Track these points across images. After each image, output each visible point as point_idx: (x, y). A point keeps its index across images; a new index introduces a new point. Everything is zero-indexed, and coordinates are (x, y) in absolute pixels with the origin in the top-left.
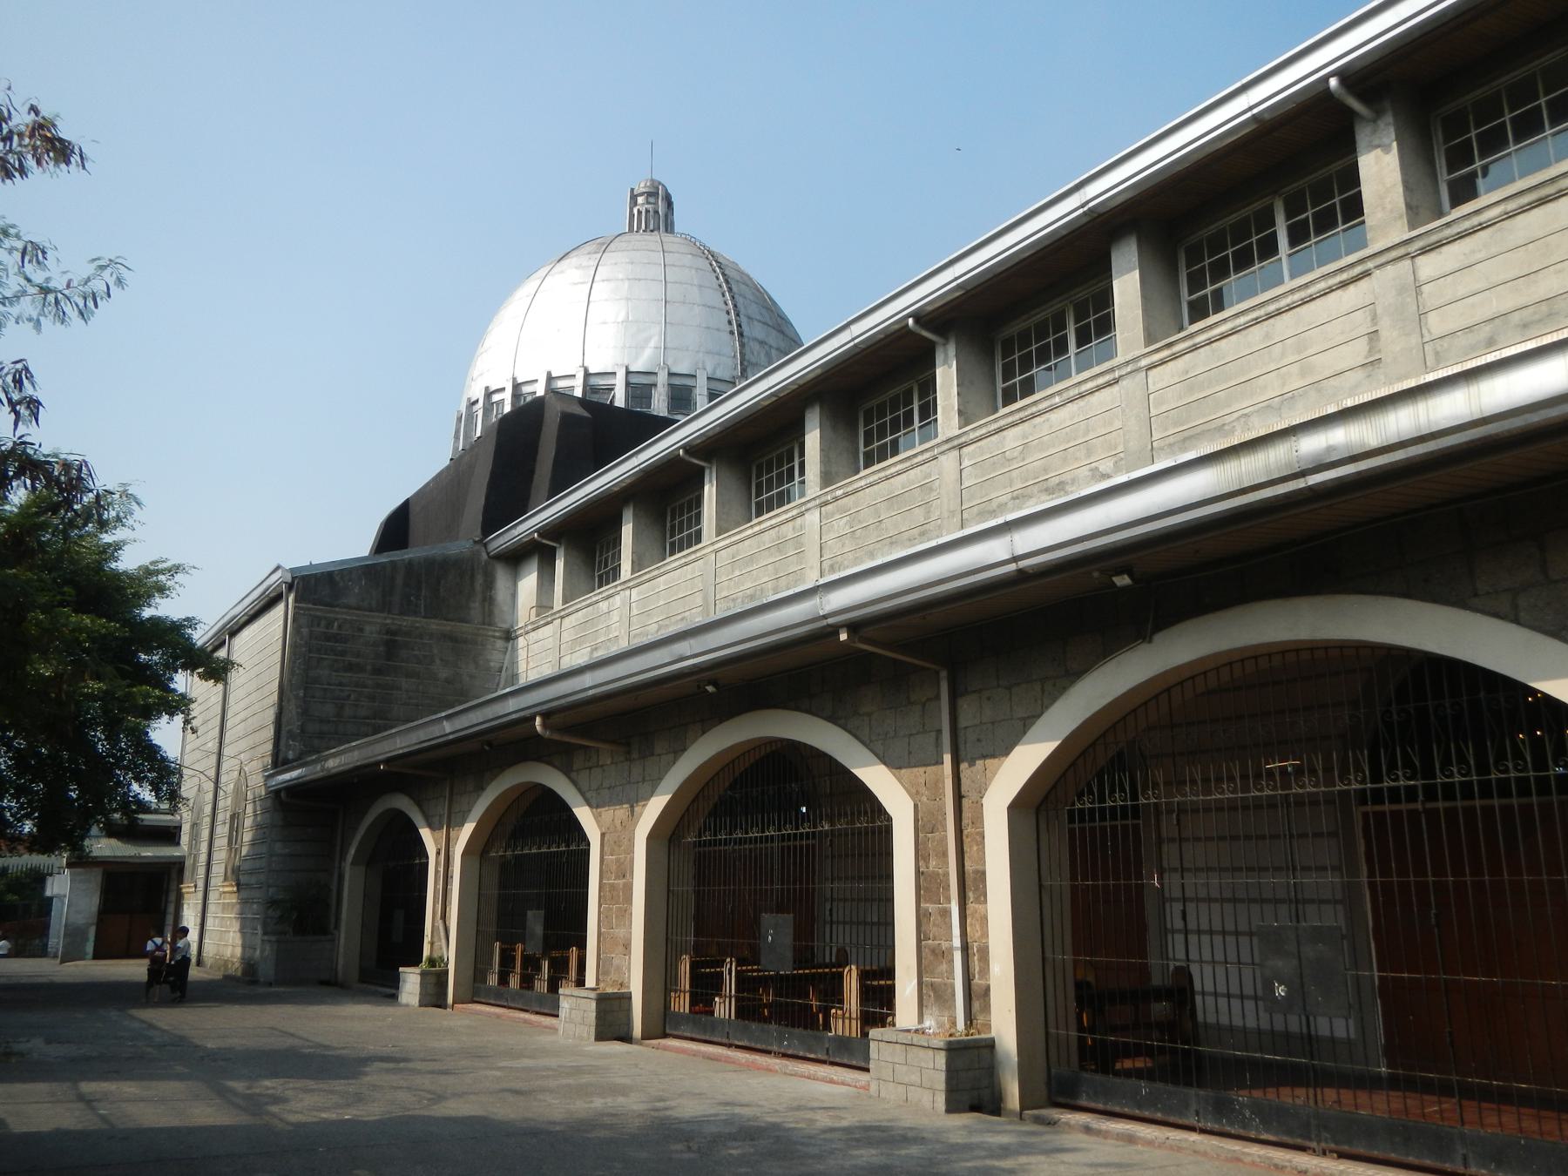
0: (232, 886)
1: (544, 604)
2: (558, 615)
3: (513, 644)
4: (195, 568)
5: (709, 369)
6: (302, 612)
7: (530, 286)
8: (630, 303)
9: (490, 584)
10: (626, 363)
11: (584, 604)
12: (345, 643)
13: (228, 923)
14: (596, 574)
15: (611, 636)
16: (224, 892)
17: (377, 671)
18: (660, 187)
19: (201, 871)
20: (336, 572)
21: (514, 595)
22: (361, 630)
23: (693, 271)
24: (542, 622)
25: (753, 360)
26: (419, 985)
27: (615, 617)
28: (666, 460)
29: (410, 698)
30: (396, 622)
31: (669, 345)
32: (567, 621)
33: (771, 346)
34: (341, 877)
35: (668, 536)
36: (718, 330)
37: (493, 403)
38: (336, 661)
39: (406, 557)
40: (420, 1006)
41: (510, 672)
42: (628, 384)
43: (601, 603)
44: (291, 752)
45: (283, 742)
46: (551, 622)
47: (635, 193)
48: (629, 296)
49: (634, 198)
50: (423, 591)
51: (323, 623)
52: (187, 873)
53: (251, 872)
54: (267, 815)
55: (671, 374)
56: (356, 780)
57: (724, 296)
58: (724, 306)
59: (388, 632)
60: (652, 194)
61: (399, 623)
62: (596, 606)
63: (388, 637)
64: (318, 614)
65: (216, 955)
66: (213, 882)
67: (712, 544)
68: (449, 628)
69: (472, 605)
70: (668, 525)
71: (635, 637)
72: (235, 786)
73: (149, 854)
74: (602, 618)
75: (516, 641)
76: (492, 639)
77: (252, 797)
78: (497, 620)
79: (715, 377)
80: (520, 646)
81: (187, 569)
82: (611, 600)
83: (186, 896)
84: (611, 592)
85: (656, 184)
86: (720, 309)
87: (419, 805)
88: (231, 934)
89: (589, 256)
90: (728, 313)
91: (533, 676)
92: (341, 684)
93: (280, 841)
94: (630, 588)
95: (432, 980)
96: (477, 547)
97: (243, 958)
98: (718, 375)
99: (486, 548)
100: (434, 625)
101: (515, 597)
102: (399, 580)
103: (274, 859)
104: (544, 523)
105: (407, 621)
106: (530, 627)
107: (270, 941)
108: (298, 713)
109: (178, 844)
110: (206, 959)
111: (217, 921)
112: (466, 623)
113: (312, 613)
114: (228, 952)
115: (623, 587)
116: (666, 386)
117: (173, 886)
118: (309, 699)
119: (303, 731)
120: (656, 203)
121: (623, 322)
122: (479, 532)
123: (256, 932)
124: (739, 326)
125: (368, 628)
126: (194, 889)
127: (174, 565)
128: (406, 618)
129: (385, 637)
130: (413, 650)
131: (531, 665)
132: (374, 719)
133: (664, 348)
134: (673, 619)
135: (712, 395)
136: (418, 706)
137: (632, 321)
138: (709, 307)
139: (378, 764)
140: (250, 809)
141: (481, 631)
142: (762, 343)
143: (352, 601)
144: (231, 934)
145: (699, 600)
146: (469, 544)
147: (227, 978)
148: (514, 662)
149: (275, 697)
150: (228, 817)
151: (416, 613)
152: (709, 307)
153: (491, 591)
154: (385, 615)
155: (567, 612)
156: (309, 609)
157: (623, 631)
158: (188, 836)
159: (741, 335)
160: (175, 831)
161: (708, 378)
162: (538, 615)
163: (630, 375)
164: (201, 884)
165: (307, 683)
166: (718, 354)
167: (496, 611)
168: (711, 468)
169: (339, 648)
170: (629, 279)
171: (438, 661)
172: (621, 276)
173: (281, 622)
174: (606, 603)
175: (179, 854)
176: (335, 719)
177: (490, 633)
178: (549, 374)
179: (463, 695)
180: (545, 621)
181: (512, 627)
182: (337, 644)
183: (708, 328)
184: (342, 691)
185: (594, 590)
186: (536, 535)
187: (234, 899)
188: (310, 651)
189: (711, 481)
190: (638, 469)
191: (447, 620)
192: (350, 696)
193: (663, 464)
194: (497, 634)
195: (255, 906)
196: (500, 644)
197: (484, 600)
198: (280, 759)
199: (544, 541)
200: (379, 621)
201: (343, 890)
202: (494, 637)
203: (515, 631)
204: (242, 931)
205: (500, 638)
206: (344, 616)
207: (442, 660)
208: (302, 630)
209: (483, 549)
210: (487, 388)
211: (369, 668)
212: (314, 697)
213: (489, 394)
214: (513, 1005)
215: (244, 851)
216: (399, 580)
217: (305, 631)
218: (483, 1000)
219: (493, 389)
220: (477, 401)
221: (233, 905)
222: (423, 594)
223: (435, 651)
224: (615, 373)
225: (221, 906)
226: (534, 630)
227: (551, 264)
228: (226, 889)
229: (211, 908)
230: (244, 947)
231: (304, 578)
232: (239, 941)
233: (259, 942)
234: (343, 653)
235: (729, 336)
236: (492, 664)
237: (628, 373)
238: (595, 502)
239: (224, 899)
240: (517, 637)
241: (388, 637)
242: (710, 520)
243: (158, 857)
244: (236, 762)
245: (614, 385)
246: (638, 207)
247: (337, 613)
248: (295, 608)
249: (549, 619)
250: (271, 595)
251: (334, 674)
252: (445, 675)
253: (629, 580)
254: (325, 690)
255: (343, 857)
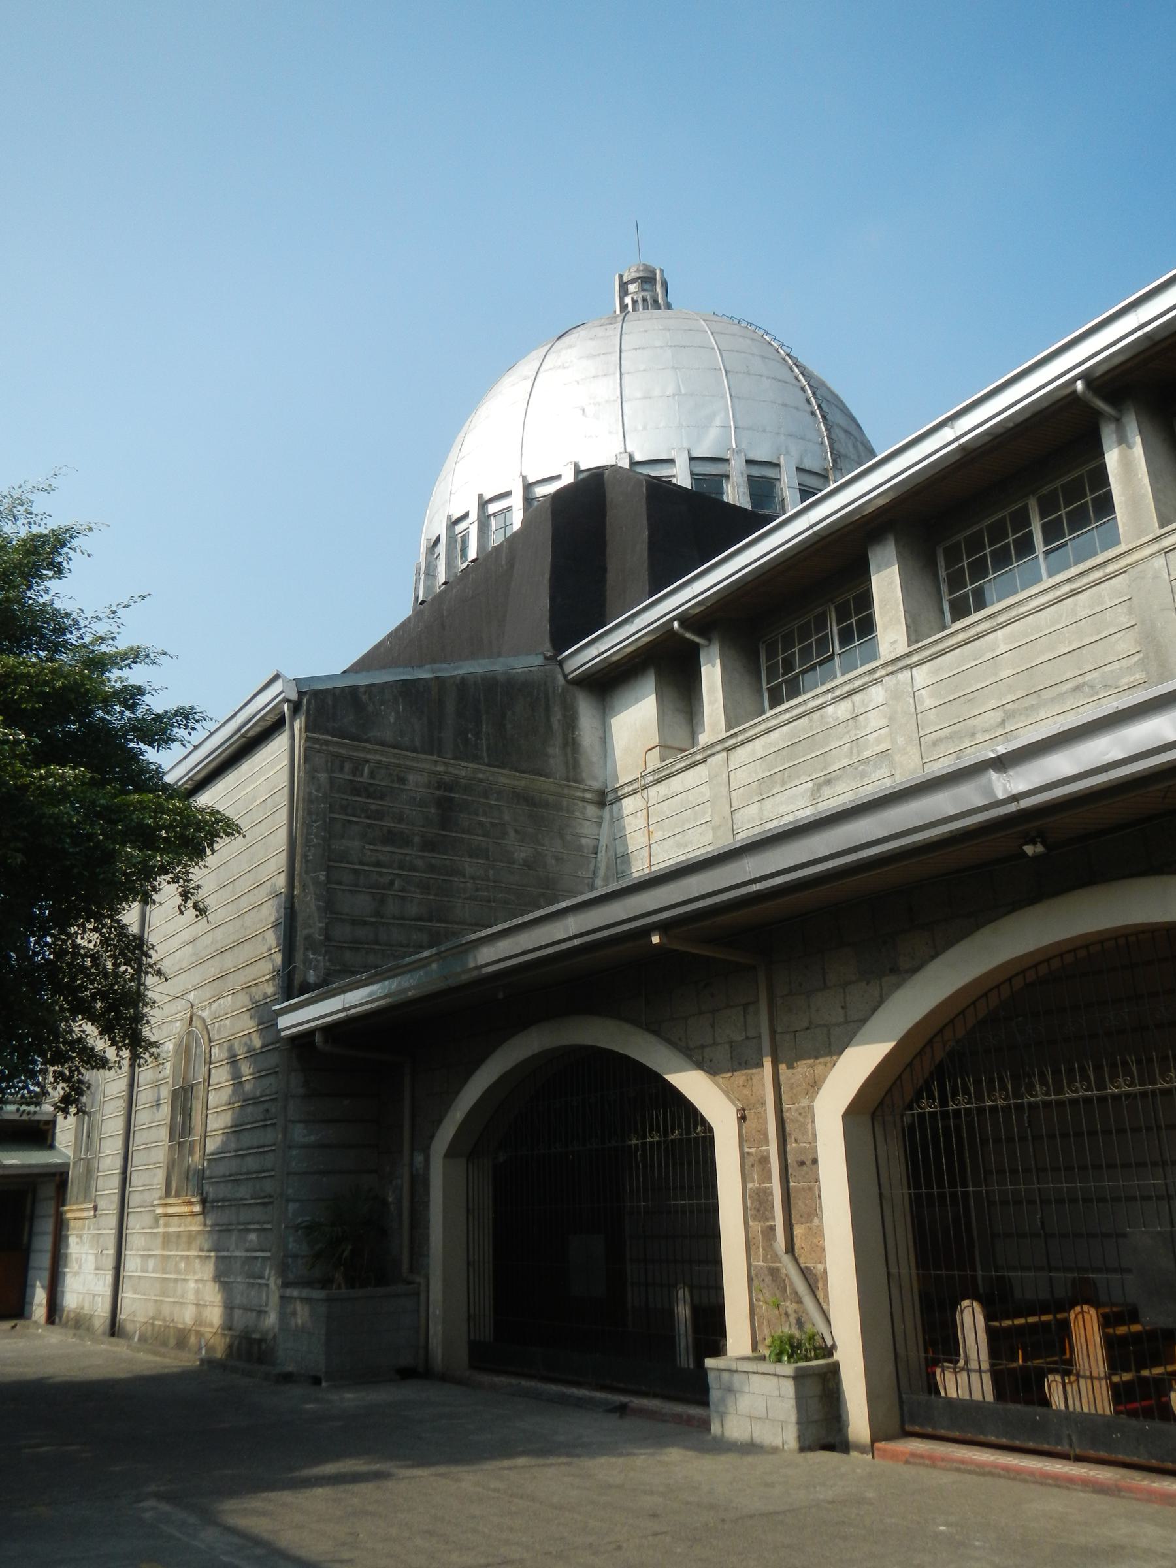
0: (190, 1204)
1: (669, 743)
2: (719, 748)
3: (611, 812)
4: (165, 654)
5: (795, 451)
6: (317, 746)
7: (526, 368)
8: (679, 373)
9: (571, 723)
10: (685, 445)
11: (787, 716)
12: (382, 799)
13: (182, 1265)
14: (765, 686)
15: (866, 754)
16: (166, 1215)
17: (429, 845)
18: (658, 272)
19: (109, 1187)
20: (362, 689)
21: (605, 739)
22: (402, 780)
23: (749, 342)
24: (683, 764)
25: (843, 451)
26: (793, 1402)
27: (875, 720)
28: (1001, 430)
29: (477, 890)
30: (451, 769)
31: (740, 424)
32: (741, 754)
33: (856, 438)
34: (420, 1184)
35: (945, 589)
36: (797, 409)
37: (489, 516)
38: (369, 826)
39: (456, 673)
40: (802, 1449)
41: (611, 853)
42: (692, 474)
43: (830, 709)
44: (312, 972)
45: (299, 956)
46: (704, 761)
47: (625, 280)
48: (676, 366)
49: (623, 287)
50: (485, 726)
51: (348, 766)
52: (73, 1190)
53: (234, 1180)
54: (271, 1080)
55: (749, 462)
56: (501, 996)
57: (792, 371)
58: (795, 382)
59: (441, 785)
60: (648, 279)
61: (456, 772)
62: (816, 716)
63: (440, 793)
64: (342, 751)
65: (154, 1318)
66: (134, 1200)
67: (1157, 539)
68: (523, 783)
69: (551, 751)
70: (943, 574)
71: (935, 744)
72: (178, 1047)
73: (14, 1162)
74: (840, 729)
75: (614, 806)
76: (581, 804)
77: (225, 1055)
78: (584, 775)
79: (803, 467)
80: (626, 812)
81: (152, 656)
82: (857, 698)
83: (72, 1224)
84: (858, 683)
85: (652, 269)
86: (793, 385)
87: (655, 1029)
88: (192, 1285)
89: (605, 327)
90: (803, 390)
91: (667, 857)
92: (378, 864)
93: (300, 1122)
94: (910, 667)
95: (814, 1388)
96: (550, 666)
97: (228, 1326)
98: (808, 464)
99: (562, 669)
100: (504, 778)
101: (605, 742)
102: (450, 707)
103: (294, 1152)
104: (699, 599)
105: (464, 770)
106: (651, 778)
107: (307, 1300)
108: (318, 908)
109: (51, 1147)
110: (129, 1327)
111: (151, 1263)
112: (546, 776)
113: (331, 749)
114: (187, 1317)
115: (890, 669)
116: (745, 475)
117: (47, 1208)
118: (333, 886)
119: (328, 938)
120: (653, 290)
121: (674, 395)
122: (548, 645)
123: (259, 1281)
124: (820, 407)
125: (411, 778)
126: (92, 1213)
127: (132, 649)
128: (463, 764)
129: (437, 792)
130: (477, 815)
131: (658, 835)
132: (430, 920)
133: (735, 428)
134: (1046, 695)
135: (805, 493)
136: (489, 901)
137: (685, 394)
138: (779, 380)
139: (647, 931)
140: (221, 1076)
141: (566, 791)
142: (846, 431)
143: (388, 735)
144: (192, 1285)
145: (1126, 644)
146: (538, 660)
147: (210, 1363)
148: (619, 837)
149: (281, 881)
150: (165, 1093)
151: (476, 758)
152: (779, 380)
153: (573, 733)
154: (435, 758)
155: (741, 738)
156: (327, 743)
157: (900, 740)
158: (73, 1131)
159: (824, 417)
160: (46, 1127)
161: (797, 468)
162: (663, 760)
163: (693, 462)
164: (109, 1207)
165: (329, 861)
166: (802, 438)
167: (583, 762)
168: (1118, 420)
169: (373, 807)
170: (671, 346)
171: (512, 834)
172: (658, 344)
173: (285, 762)
174: (845, 707)
175: (59, 1161)
176: (373, 919)
177: (579, 794)
178: (576, 465)
179: (549, 890)
180: (688, 762)
181: (606, 787)
182: (369, 801)
183: (785, 405)
184: (380, 874)
185: (763, 713)
186: (676, 624)
187: (195, 1226)
188: (332, 812)
189: (1122, 440)
190: (955, 445)
191: (524, 772)
192: (392, 883)
193: (1017, 426)
194: (588, 796)
195: (253, 1237)
196: (591, 810)
197: (565, 744)
198: (296, 983)
199: (688, 635)
200: (427, 766)
201: (426, 1205)
202: (583, 800)
203: (615, 790)
204: (220, 1278)
205: (591, 802)
206: (378, 757)
207: (516, 831)
208: (319, 775)
209: (558, 669)
210: (481, 496)
211: (417, 839)
212: (340, 883)
213: (483, 504)
214: (1092, 1453)
215: (212, 1145)
216: (450, 707)
217: (323, 777)
218: (943, 1432)
219: (487, 497)
220: (466, 516)
221: (191, 1237)
222: (484, 730)
223: (507, 817)
224: (671, 461)
225: (159, 1240)
226: (658, 781)
227: (546, 344)
228: (171, 1210)
229: (136, 1241)
230: (229, 1307)
231: (316, 693)
232: (213, 1297)
233: (274, 1299)
234: (379, 815)
235: (810, 418)
236: (584, 841)
237: (691, 459)
238: (823, 538)
239: (166, 1225)
240: (619, 799)
241: (440, 793)
242: (1134, 502)
243: (30, 1166)
244: (181, 1004)
245: (674, 476)
246: (631, 296)
247: (369, 751)
248: (307, 739)
249: (698, 757)
250: (250, 734)
251: (367, 846)
252: (523, 855)
253: (908, 655)
254: (356, 872)
255: (423, 1144)
